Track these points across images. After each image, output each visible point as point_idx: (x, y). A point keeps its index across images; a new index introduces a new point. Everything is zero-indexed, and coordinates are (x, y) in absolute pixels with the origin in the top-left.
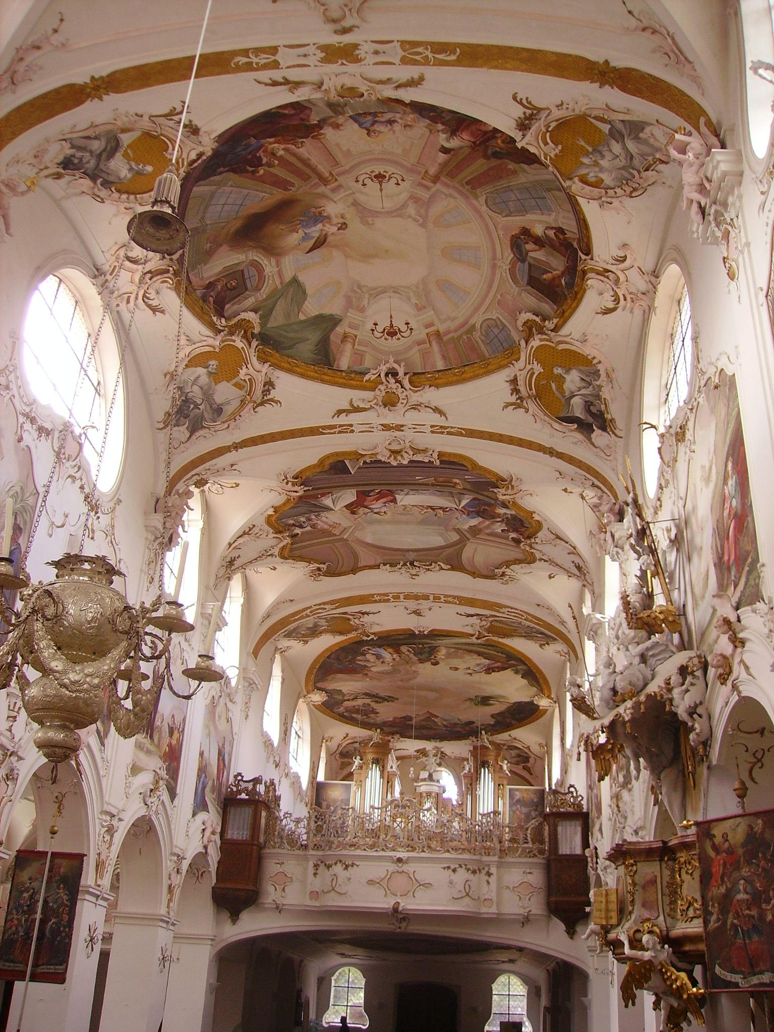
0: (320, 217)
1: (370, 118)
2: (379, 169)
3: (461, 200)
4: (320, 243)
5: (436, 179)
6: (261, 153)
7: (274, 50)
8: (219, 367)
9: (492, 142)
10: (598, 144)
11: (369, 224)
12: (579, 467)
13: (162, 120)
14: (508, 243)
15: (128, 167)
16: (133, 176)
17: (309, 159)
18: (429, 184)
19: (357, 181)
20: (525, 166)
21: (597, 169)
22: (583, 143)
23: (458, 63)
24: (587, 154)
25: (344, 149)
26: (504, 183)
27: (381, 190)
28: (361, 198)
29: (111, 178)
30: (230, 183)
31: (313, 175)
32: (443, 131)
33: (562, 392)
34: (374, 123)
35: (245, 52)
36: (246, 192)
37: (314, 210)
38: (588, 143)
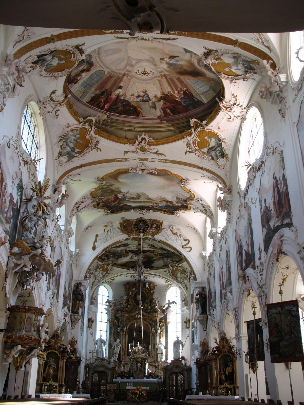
0: (170, 65)
1: (145, 99)
2: (145, 77)
3: (114, 69)
4: (172, 57)
5: (124, 75)
6: (182, 96)
7: (159, 162)
8: (225, 68)
9: (105, 98)
10: (77, 144)
11: (151, 58)
12: (35, 42)
13: (194, 151)
14: (94, 63)
15: (211, 141)
16: (212, 137)
17: (168, 85)
18: (126, 72)
19: (153, 73)
20: (93, 95)
21: (74, 135)
22: (81, 141)
23: (116, 159)
24: (78, 138)
25: (155, 86)
26: (99, 83)
27: (145, 69)
28: (153, 67)
29: (217, 141)
30: (196, 92)
31: (168, 79)
32: (121, 96)
33: (57, 57)
34: (143, 97)
35: (166, 162)
36: (192, 85)
37: (172, 68)
38: (79, 142)
